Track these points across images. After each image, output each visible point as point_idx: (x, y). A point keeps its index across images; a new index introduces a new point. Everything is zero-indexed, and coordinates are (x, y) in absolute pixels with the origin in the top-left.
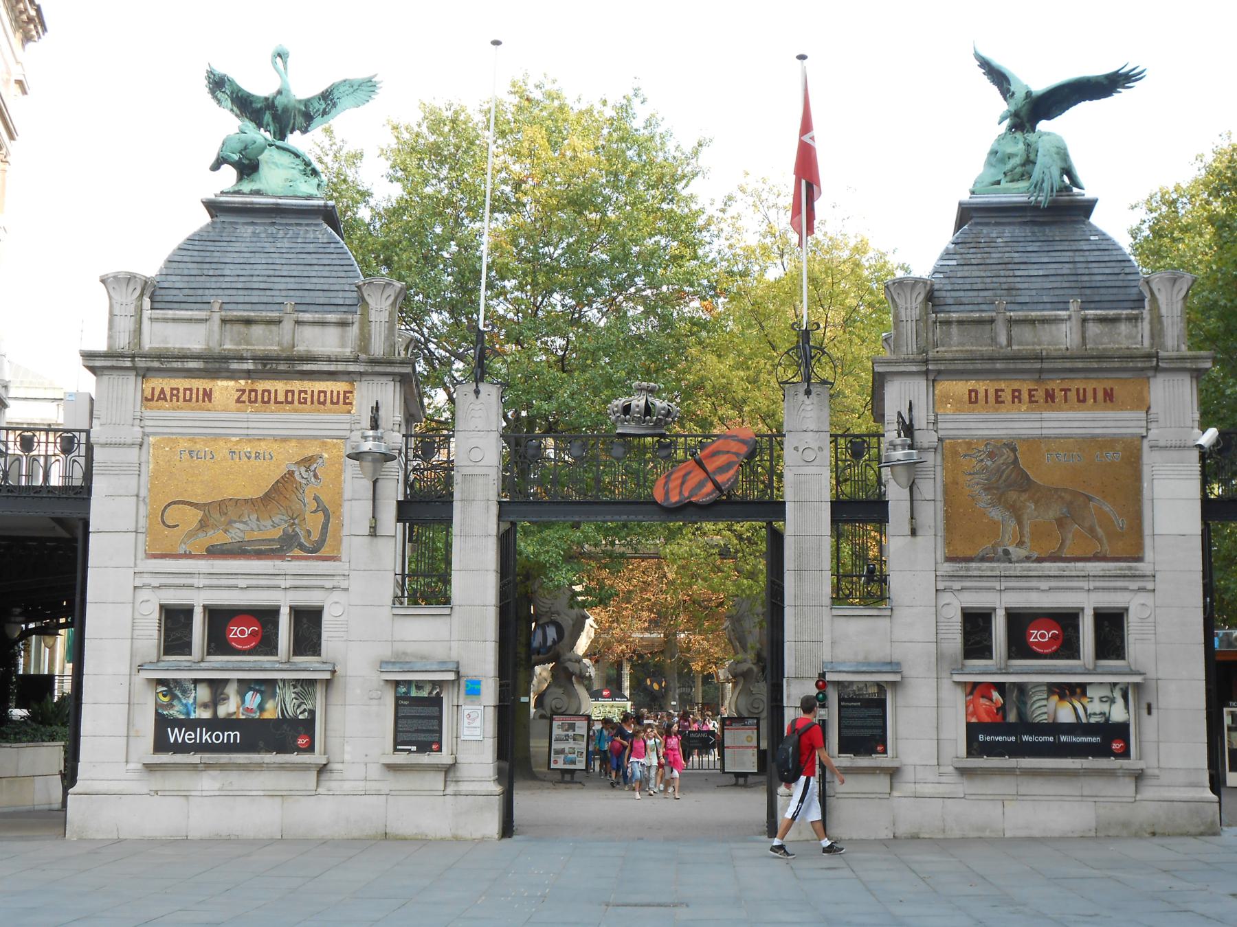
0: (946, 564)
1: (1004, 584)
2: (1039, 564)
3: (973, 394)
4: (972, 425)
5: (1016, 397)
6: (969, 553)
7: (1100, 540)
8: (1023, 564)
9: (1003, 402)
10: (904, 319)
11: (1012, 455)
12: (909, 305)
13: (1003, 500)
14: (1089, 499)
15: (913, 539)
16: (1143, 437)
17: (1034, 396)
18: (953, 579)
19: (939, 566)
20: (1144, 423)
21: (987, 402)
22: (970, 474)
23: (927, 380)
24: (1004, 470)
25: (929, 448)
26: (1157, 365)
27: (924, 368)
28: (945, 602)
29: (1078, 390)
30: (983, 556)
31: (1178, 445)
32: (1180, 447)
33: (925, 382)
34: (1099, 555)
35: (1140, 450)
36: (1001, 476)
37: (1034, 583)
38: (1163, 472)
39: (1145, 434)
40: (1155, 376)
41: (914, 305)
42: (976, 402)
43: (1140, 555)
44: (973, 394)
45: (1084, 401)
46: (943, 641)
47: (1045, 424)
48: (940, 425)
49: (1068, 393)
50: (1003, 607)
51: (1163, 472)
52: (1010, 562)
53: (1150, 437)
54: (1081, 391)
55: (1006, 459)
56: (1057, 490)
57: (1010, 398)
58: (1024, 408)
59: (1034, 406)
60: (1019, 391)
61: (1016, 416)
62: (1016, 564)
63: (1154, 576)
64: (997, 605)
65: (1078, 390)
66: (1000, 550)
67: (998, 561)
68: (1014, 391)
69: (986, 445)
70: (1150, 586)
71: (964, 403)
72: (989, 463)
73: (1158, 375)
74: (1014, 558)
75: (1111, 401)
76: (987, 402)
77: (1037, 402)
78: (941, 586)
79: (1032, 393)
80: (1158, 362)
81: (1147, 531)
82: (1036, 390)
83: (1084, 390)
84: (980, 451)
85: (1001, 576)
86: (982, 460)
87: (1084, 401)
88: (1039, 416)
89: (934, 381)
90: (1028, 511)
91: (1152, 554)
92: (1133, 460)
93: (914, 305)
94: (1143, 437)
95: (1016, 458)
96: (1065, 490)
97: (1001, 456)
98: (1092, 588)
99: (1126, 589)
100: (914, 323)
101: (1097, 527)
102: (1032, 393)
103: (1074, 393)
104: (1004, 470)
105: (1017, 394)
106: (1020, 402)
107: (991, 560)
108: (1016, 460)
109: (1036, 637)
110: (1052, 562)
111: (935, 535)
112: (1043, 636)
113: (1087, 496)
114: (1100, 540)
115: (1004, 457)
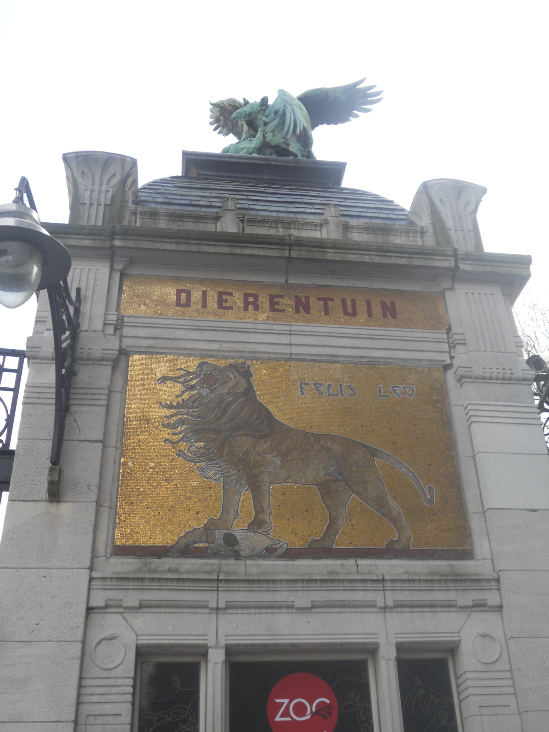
0: (113, 560)
1: (224, 598)
2: (290, 562)
3: (183, 296)
4: (179, 334)
5: (251, 303)
6: (159, 540)
7: (395, 521)
8: (261, 562)
9: (230, 308)
10: (87, 201)
11: (243, 381)
12: (96, 188)
13: (226, 450)
14: (374, 453)
15: (53, 508)
16: (447, 367)
17: (277, 303)
18: (126, 584)
19: (100, 561)
20: (446, 347)
21: (204, 306)
22: (171, 407)
23: (112, 269)
24: (230, 404)
25: (102, 359)
26: (457, 267)
27: (108, 244)
28: (103, 635)
29: (344, 301)
30: (187, 546)
31: (501, 376)
32: (504, 379)
33: (107, 270)
34: (396, 546)
35: (444, 384)
36: (223, 413)
37: (282, 596)
38: (486, 414)
39: (448, 362)
40: (452, 289)
41: (104, 188)
42: (188, 304)
43: (466, 547)
44: (183, 296)
45: (354, 314)
46: (91, 720)
47: (295, 340)
48: (126, 331)
49: (330, 303)
50: (222, 643)
51: (486, 414)
52: (237, 556)
53: (456, 362)
54: (349, 304)
55: (233, 387)
56: (318, 437)
57: (241, 304)
58: (262, 317)
59: (277, 315)
60: (256, 297)
61: (251, 326)
62: (249, 562)
63: (498, 581)
64: (211, 642)
65: (344, 301)
66: (219, 535)
67: (215, 555)
68: (246, 296)
69: (201, 365)
70: (492, 599)
71: (169, 305)
72: (205, 392)
73: (457, 286)
74: (244, 548)
75: (394, 316)
76: (204, 306)
77: (283, 311)
78: (98, 600)
79: (276, 300)
80: (456, 262)
81: (472, 506)
82: (282, 297)
83: (353, 301)
84: (189, 373)
85: (219, 581)
86: (192, 387)
87: (354, 314)
88: (287, 328)
89: (123, 275)
90: (270, 469)
91: (486, 544)
92: (435, 397)
93: (104, 188)
94: (447, 367)
95: (250, 387)
96: (332, 438)
97: (226, 382)
98: (390, 603)
99: (449, 606)
100: (102, 208)
101: (390, 499)
102: (276, 300)
103: (338, 302)
104: (230, 404)
105: (251, 299)
106: (256, 309)
107: (201, 554)
108: (249, 391)
109: (286, 713)
110: (315, 558)
111: (99, 505)
112: (300, 710)
113: (368, 448)
114: (395, 521)
115: (231, 384)
